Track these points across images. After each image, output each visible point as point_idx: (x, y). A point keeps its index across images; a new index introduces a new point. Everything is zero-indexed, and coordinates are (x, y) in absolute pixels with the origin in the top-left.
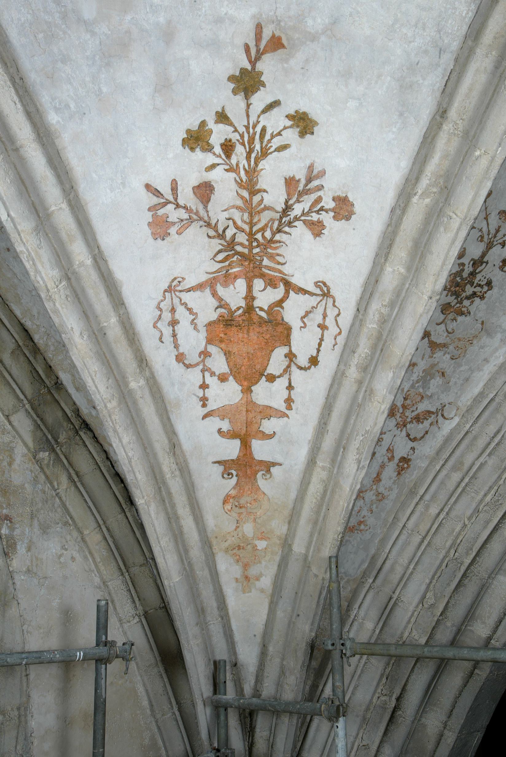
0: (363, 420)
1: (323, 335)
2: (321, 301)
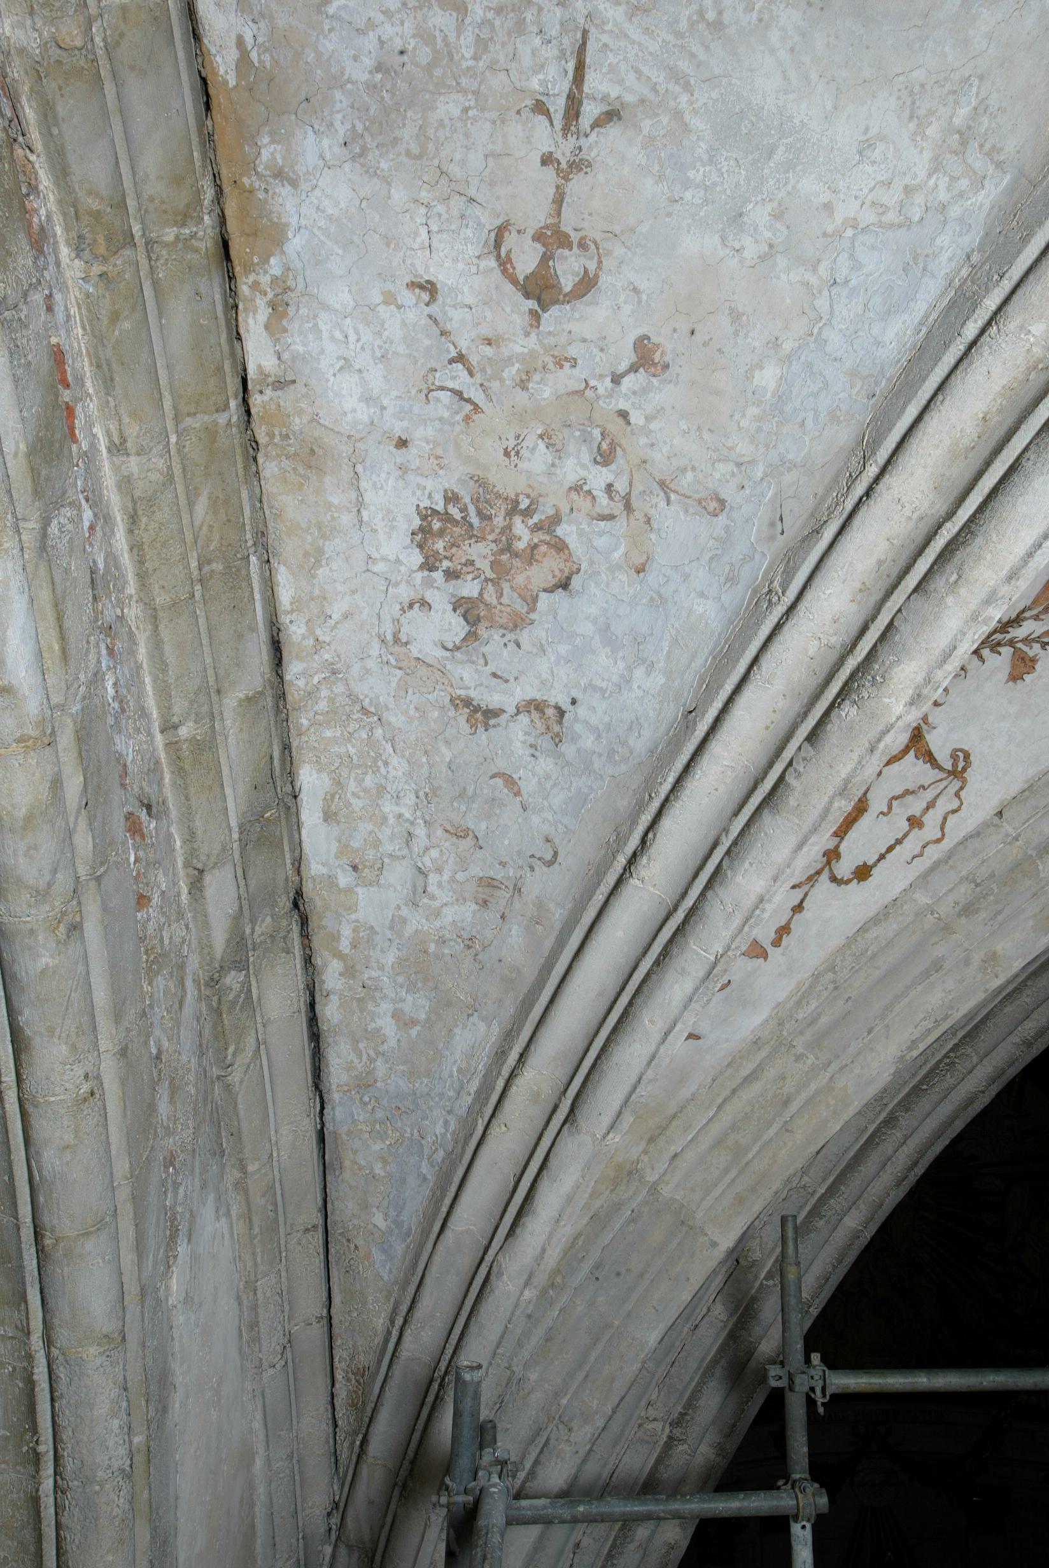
1: (905, 835)
2: (941, 780)
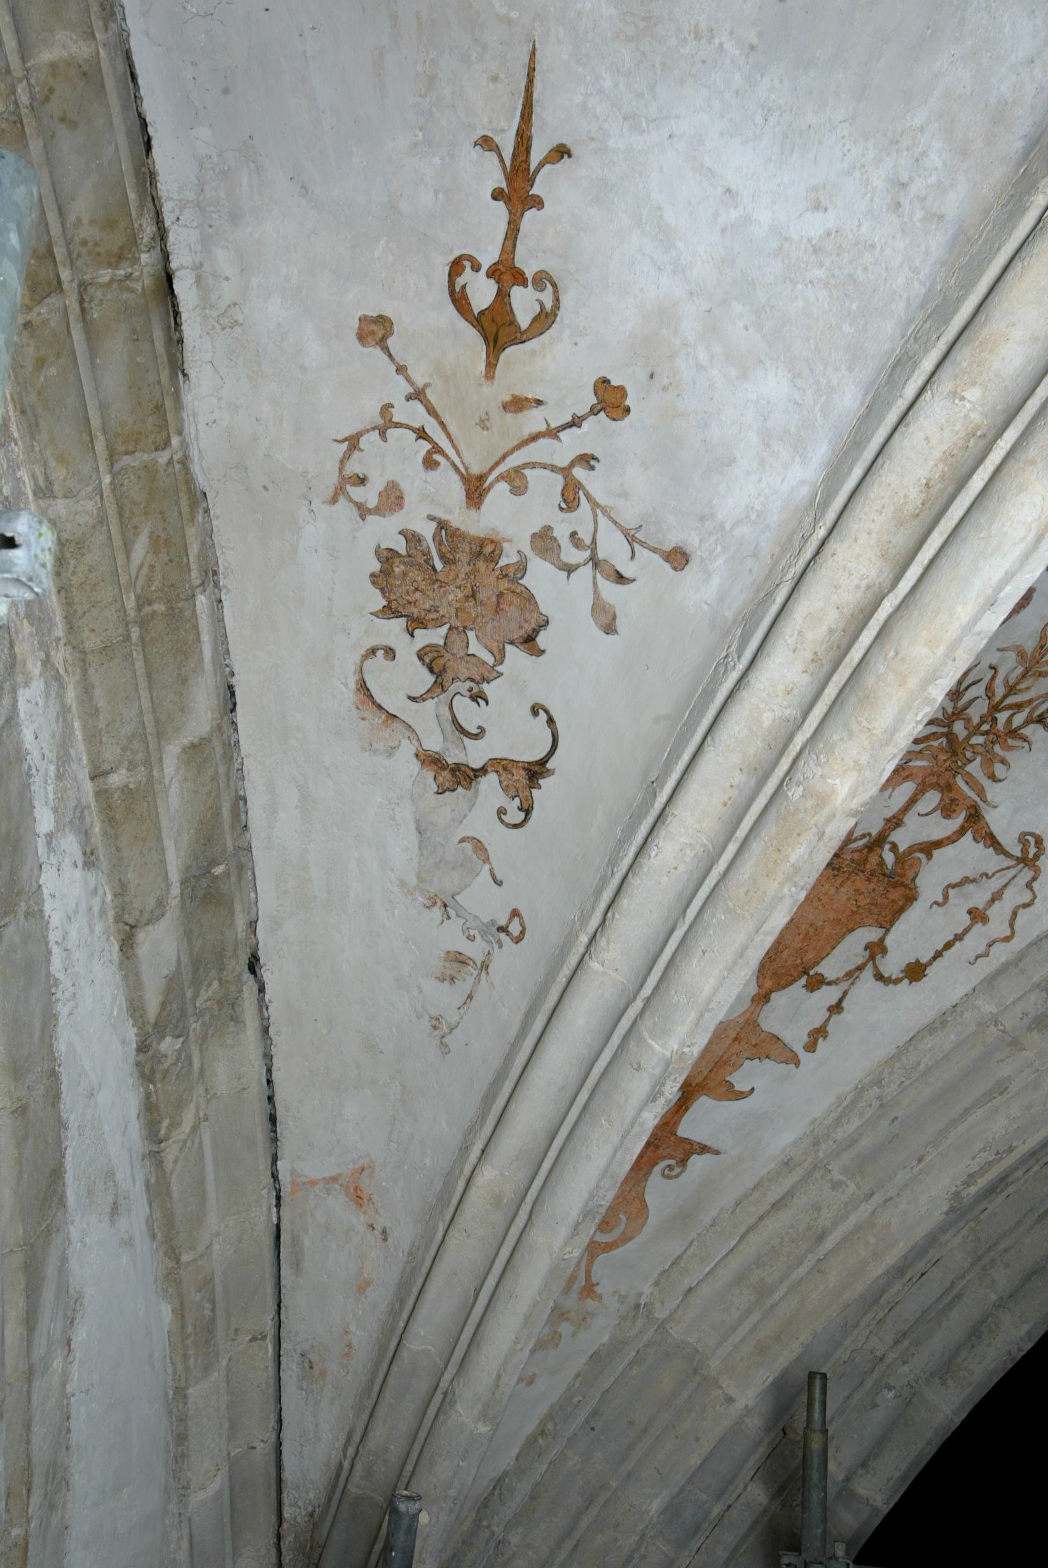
0: (1015, 1126)
1: (967, 930)
2: (1008, 868)
